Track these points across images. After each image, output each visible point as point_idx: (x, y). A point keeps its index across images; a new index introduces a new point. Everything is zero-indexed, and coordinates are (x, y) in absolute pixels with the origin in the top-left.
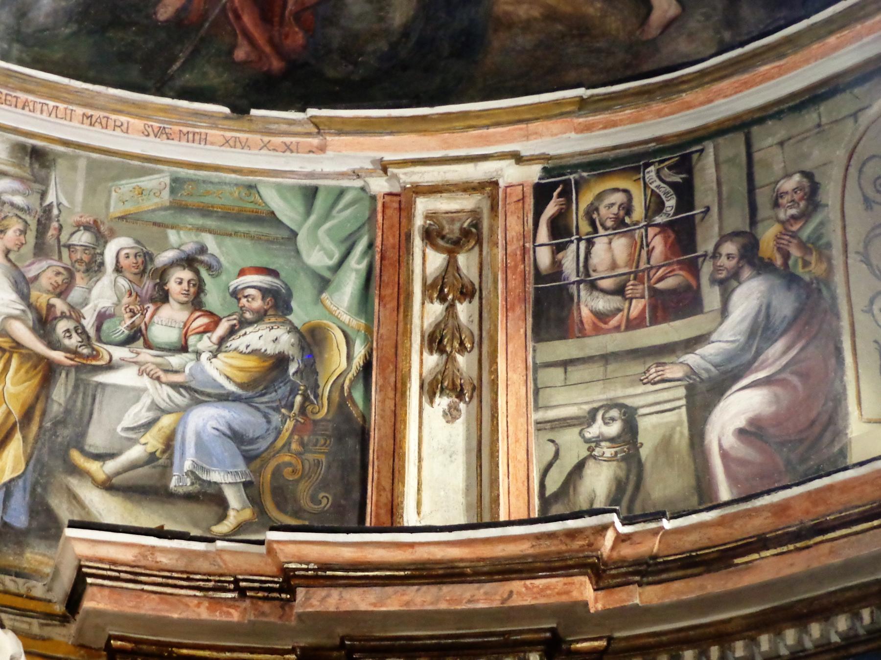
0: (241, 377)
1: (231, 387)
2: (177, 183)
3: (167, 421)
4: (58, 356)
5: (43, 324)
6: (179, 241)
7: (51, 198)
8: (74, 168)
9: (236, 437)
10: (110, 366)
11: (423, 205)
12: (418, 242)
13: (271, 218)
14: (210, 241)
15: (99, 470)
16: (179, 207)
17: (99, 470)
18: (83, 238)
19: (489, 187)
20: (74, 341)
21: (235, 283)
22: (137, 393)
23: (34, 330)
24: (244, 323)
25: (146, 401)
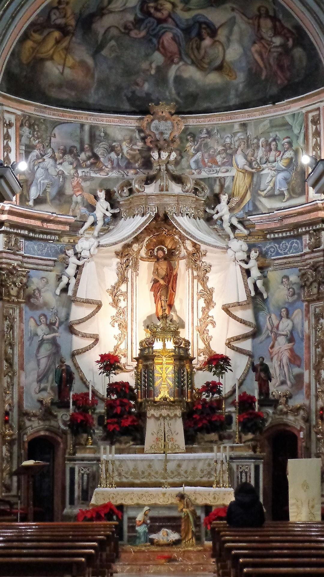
0: (285, 165)
1: (284, 168)
2: (271, 121)
3: (274, 179)
4: (254, 170)
5: (250, 165)
6: (273, 135)
7: (248, 134)
8: (251, 125)
9: (285, 179)
10: (263, 170)
11: (310, 115)
12: (310, 124)
13: (287, 124)
14: (277, 133)
15: (263, 193)
16: (272, 127)
17: (263, 193)
18: (255, 141)
19: (318, 109)
20: (256, 167)
21: (283, 143)
22: (268, 174)
23: (249, 166)
24: (285, 151)
25: (270, 175)
